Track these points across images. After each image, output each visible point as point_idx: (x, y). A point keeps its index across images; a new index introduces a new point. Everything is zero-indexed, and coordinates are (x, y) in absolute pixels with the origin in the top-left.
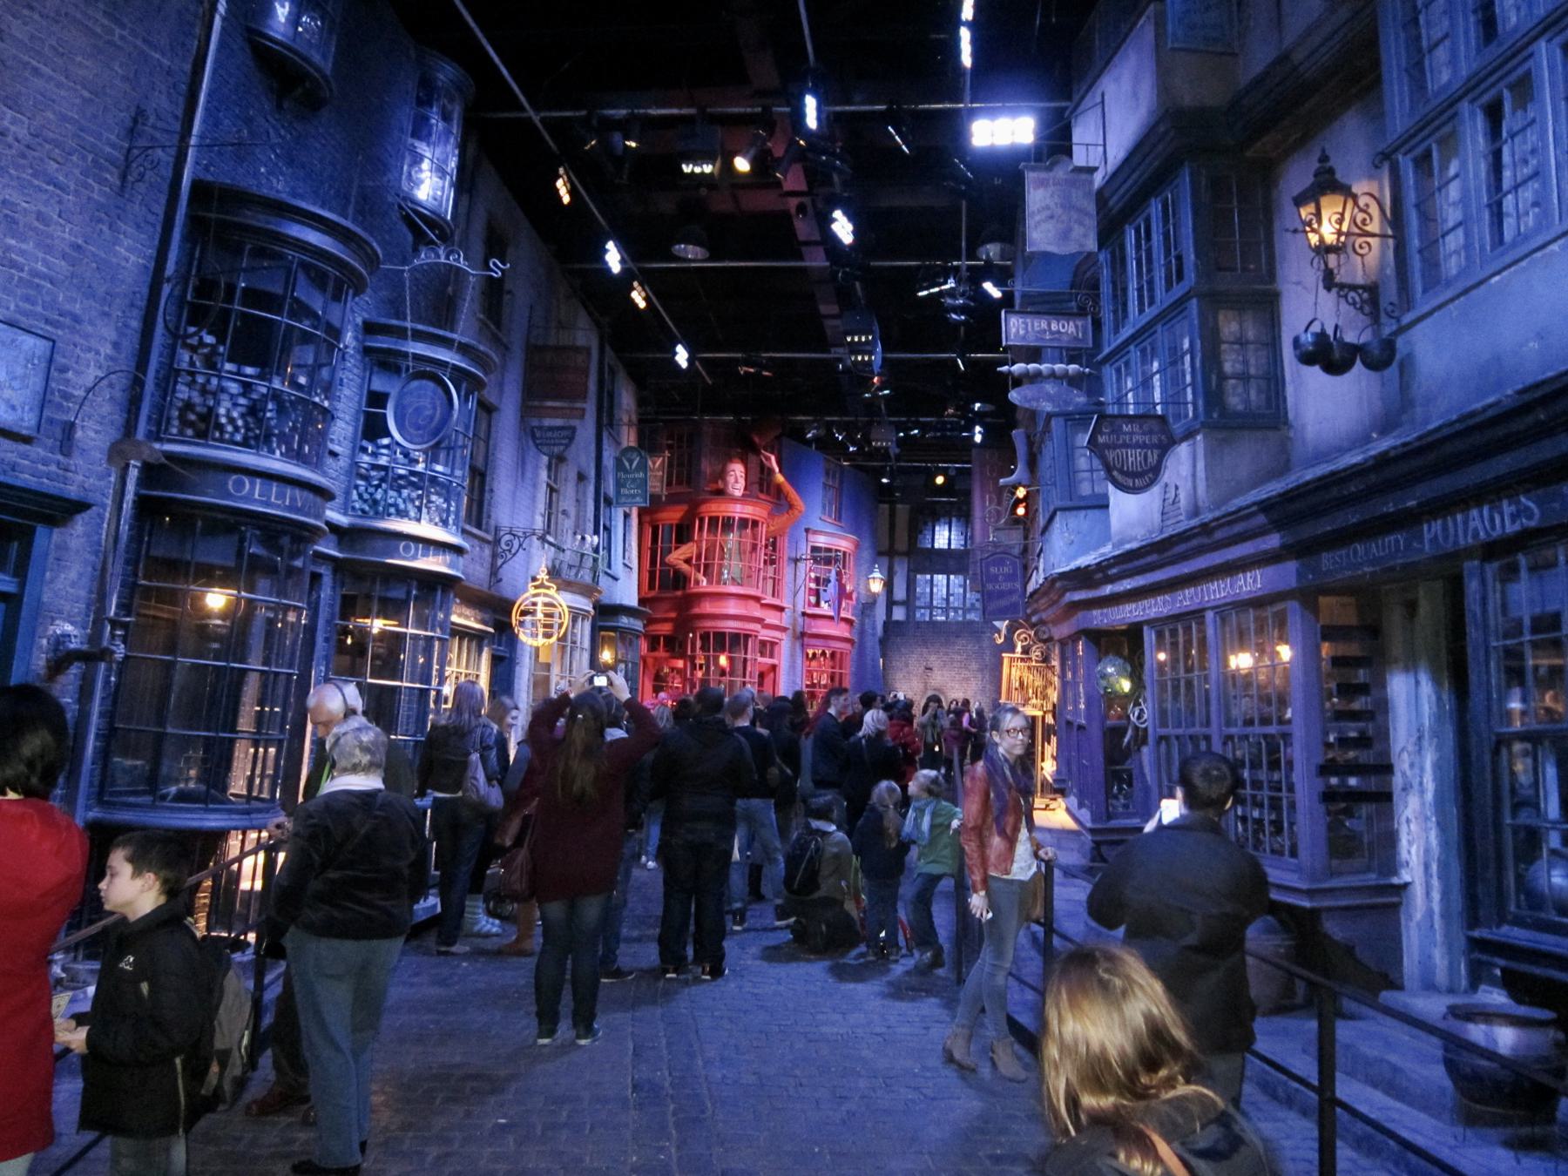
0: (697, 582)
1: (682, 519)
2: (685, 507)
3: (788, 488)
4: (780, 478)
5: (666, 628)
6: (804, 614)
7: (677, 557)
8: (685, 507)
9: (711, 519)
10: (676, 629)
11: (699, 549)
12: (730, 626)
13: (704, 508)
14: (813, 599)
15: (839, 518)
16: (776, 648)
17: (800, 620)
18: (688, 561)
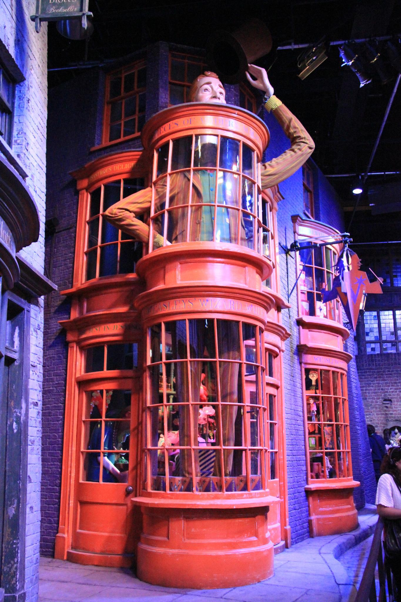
0: (157, 246)
1: (132, 171)
2: (136, 154)
3: (287, 114)
4: (275, 102)
5: (112, 331)
6: (300, 323)
7: (126, 207)
8: (136, 154)
9: (176, 142)
10: (127, 329)
11: (161, 197)
12: (217, 307)
13: (166, 129)
14: (305, 306)
15: (317, 218)
16: (275, 361)
17: (295, 329)
18: (143, 215)
